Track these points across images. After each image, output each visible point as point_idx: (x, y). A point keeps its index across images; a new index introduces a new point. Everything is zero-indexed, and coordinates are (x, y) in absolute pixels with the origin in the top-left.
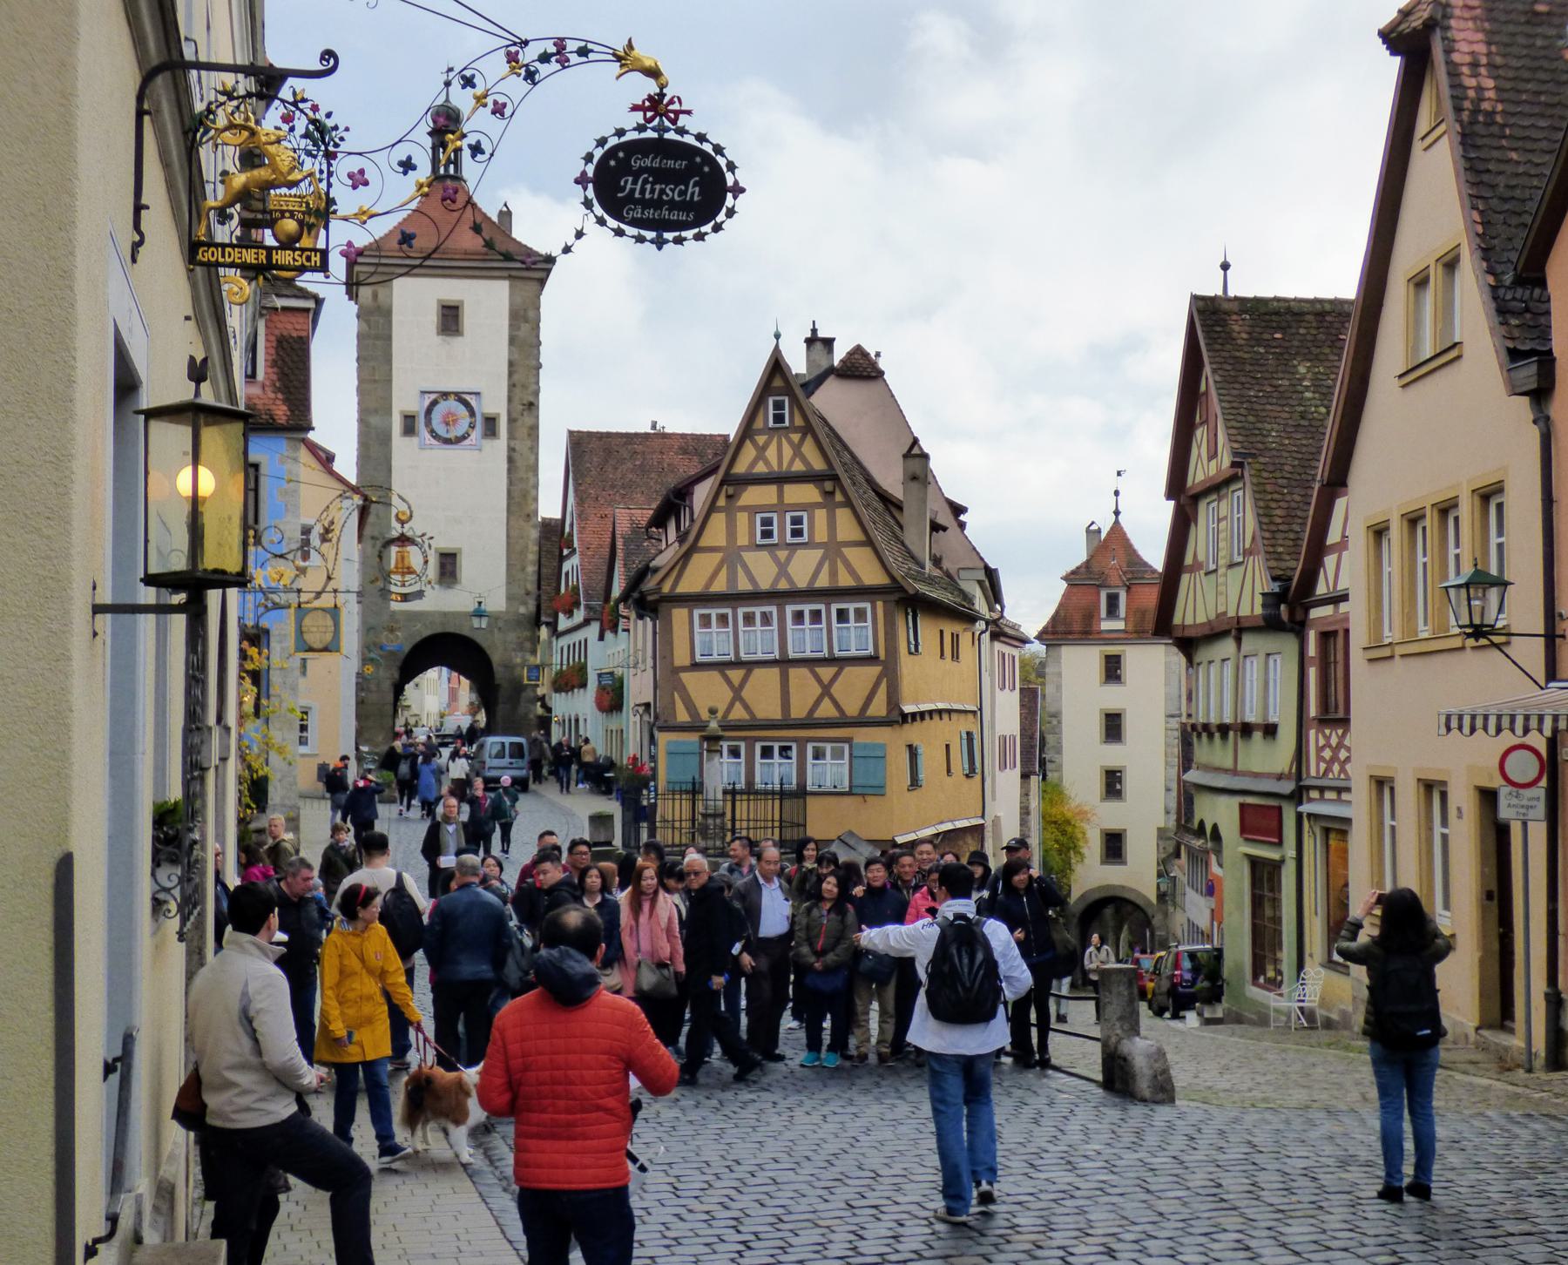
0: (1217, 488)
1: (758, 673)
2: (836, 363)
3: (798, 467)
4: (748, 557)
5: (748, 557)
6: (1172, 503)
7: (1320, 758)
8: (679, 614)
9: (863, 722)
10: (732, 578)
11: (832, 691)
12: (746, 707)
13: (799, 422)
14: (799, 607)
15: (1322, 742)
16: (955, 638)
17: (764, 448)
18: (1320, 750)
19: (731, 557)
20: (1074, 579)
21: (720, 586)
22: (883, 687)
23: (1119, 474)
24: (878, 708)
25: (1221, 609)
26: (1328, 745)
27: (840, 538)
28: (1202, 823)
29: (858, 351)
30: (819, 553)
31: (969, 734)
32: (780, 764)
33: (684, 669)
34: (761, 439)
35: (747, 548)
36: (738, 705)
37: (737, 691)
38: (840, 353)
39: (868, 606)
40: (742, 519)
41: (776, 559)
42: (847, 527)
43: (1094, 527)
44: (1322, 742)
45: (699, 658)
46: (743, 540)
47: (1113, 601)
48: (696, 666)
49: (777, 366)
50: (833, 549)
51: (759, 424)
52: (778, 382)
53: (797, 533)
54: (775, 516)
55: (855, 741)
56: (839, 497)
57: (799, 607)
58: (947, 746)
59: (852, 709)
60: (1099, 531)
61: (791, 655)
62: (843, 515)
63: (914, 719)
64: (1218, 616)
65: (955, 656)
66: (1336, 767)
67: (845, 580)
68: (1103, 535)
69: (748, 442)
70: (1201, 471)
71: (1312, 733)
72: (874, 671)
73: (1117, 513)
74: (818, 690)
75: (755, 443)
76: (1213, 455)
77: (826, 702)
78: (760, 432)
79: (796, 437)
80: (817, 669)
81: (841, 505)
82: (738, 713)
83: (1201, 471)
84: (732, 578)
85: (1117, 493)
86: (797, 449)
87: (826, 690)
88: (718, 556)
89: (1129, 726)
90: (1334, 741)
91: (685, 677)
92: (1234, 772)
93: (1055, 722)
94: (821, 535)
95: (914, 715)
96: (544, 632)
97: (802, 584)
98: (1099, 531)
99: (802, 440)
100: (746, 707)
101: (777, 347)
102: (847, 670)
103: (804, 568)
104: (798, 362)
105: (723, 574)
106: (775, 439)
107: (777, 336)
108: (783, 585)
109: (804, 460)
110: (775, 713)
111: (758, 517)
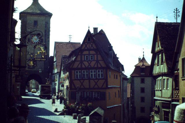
0: (160, 52)
2: (98, 32)
3: (92, 48)
4: (85, 62)
5: (85, 62)
6: (152, 54)
7: (175, 95)
8: (73, 71)
9: (102, 88)
10: (81, 65)
12: (83, 86)
13: (92, 41)
15: (175, 92)
16: (117, 76)
18: (175, 94)
19: (81, 62)
20: (137, 67)
21: (79, 67)
22: (105, 83)
23: (143, 49)
24: (105, 86)
25: (160, 71)
26: (176, 93)
28: (157, 105)
29: (102, 31)
30: (95, 62)
31: (119, 91)
34: (86, 44)
35: (84, 61)
36: (82, 86)
37: (82, 84)
38: (99, 31)
40: (83, 56)
41: (88, 63)
42: (100, 58)
43: (140, 58)
44: (175, 92)
46: (83, 59)
48: (76, 80)
49: (89, 32)
50: (97, 61)
51: (86, 41)
53: (91, 59)
58: (116, 93)
59: (100, 86)
60: (140, 58)
62: (99, 56)
63: (110, 88)
64: (159, 72)
65: (117, 78)
66: (178, 96)
67: (99, 66)
68: (141, 59)
69: (84, 44)
70: (157, 49)
71: (174, 91)
72: (104, 81)
73: (144, 55)
76: (158, 47)
77: (96, 85)
78: (86, 43)
79: (92, 43)
81: (98, 54)
82: (82, 87)
83: (157, 49)
84: (81, 65)
85: (143, 52)
86: (92, 46)
87: (96, 84)
88: (79, 62)
89: (146, 90)
90: (177, 92)
92: (162, 97)
94: (95, 59)
95: (110, 87)
96: (50, 74)
98: (140, 58)
99: (93, 44)
100: (83, 86)
101: (89, 30)
103: (93, 64)
104: (92, 31)
105: (80, 65)
107: (89, 27)
108: (89, 67)
109: (93, 47)
110: (88, 87)
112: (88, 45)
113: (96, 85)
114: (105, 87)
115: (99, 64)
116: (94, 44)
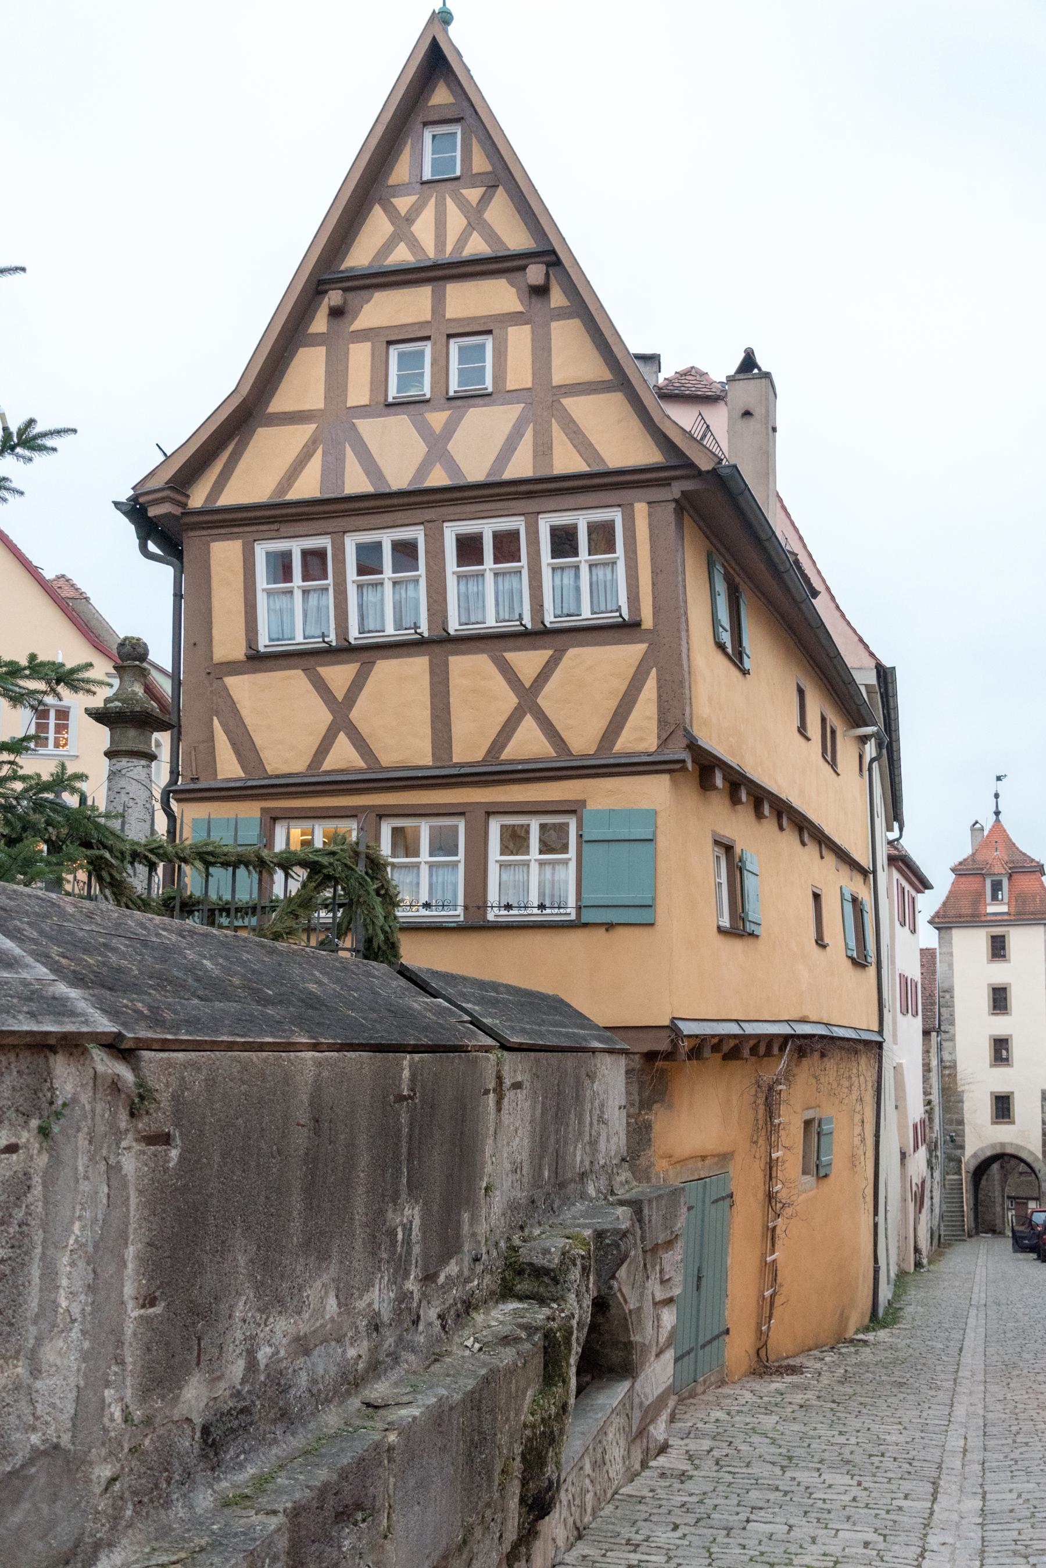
1: (385, 668)
3: (477, 246)
11: (539, 700)
13: (480, 163)
14: (468, 527)
17: (410, 219)
27: (557, 379)
30: (515, 410)
32: (432, 866)
33: (233, 668)
34: (403, 204)
36: (342, 740)
39: (616, 516)
40: (360, 355)
41: (424, 430)
45: (263, 643)
47: (997, 887)
52: (441, 96)
54: (428, 348)
55: (591, 806)
56: (557, 298)
57: (468, 527)
61: (454, 626)
69: (378, 212)
72: (632, 652)
74: (510, 700)
75: (391, 212)
77: (529, 722)
78: (401, 190)
79: (473, 195)
80: (509, 656)
81: (561, 314)
86: (475, 220)
91: (239, 686)
93: (948, 996)
97: (475, 472)
99: (485, 201)
102: (572, 652)
105: (314, 469)
106: (433, 201)
108: (438, 478)
109: (490, 236)
111: (394, 352)
112: (428, 216)
113: (529, 722)
114: (650, 743)
115: (558, 435)
116: (501, 193)
